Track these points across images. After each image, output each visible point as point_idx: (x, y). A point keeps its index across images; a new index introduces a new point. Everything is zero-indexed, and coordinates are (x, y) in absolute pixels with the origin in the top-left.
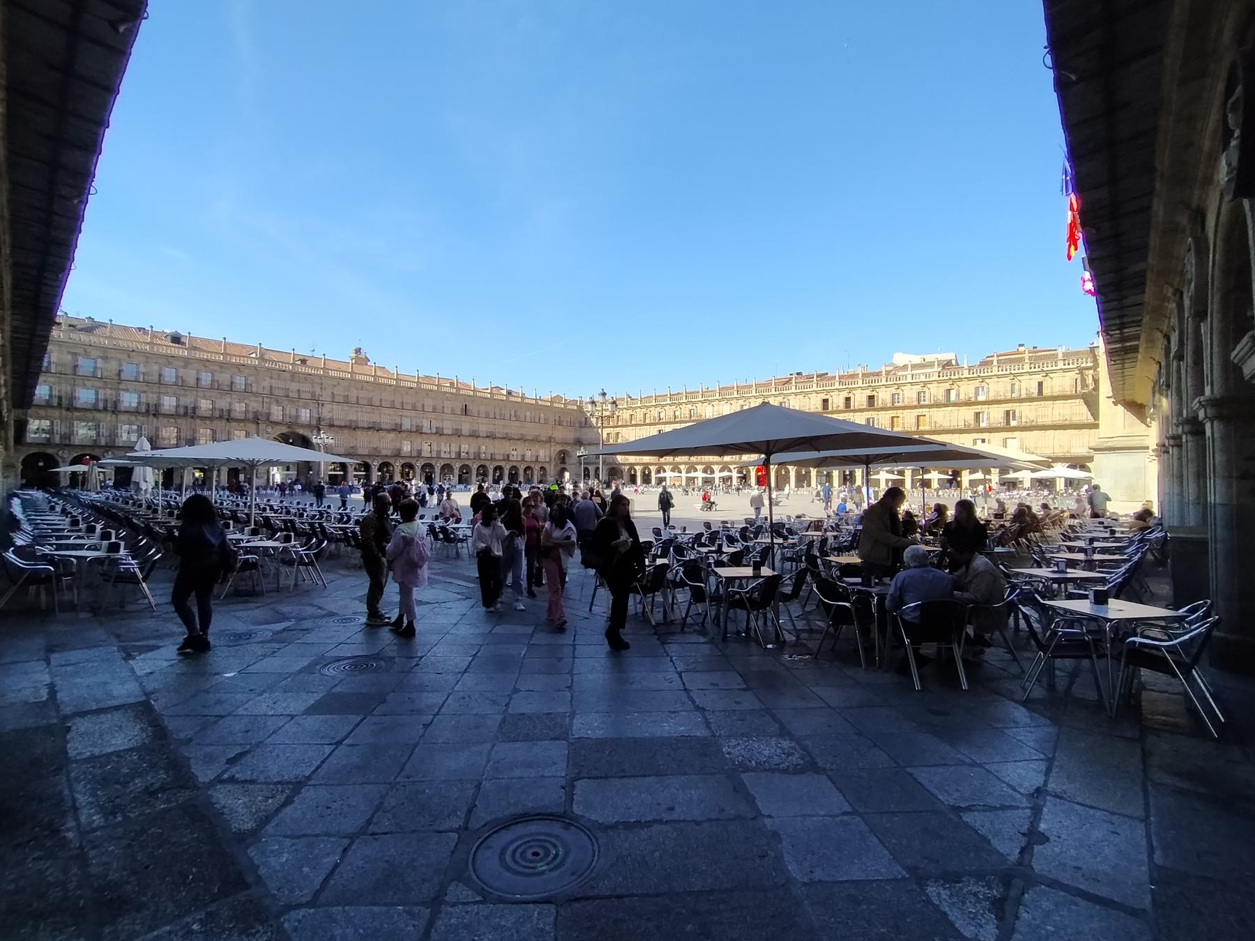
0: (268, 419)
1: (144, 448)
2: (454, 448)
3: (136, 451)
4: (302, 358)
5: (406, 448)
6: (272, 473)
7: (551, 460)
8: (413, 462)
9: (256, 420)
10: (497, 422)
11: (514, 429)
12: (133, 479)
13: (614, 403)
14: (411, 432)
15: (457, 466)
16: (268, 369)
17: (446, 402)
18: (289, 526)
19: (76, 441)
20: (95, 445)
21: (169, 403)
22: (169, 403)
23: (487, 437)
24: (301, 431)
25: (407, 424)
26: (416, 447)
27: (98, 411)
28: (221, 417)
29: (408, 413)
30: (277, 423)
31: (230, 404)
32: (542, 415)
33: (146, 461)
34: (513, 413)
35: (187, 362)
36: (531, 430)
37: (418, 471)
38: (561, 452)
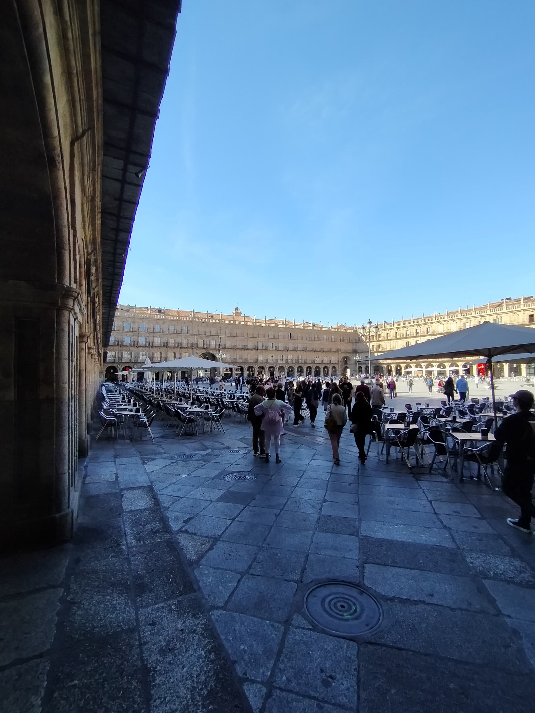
0: (197, 346)
1: (148, 364)
2: (285, 358)
3: (145, 364)
4: (211, 315)
5: (261, 358)
6: (199, 373)
7: (338, 362)
8: (264, 365)
9: (192, 347)
10: (307, 342)
11: (317, 345)
12: (144, 378)
13: (377, 327)
14: (263, 349)
15: (286, 367)
16: (197, 322)
17: (280, 332)
18: (207, 400)
19: (124, 360)
20: (131, 362)
21: (157, 341)
22: (157, 341)
23: (303, 350)
24: (211, 352)
25: (260, 346)
26: (266, 358)
27: (131, 346)
28: (178, 347)
29: (261, 340)
30: (201, 348)
31: (181, 340)
32: (333, 337)
33: (149, 369)
34: (316, 336)
35: (164, 321)
36: (326, 346)
37: (267, 370)
38: (344, 358)
